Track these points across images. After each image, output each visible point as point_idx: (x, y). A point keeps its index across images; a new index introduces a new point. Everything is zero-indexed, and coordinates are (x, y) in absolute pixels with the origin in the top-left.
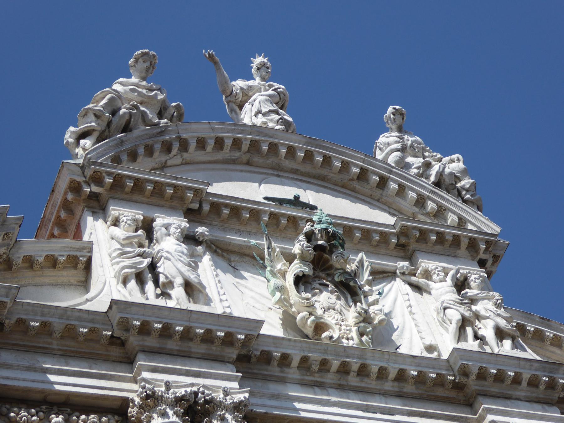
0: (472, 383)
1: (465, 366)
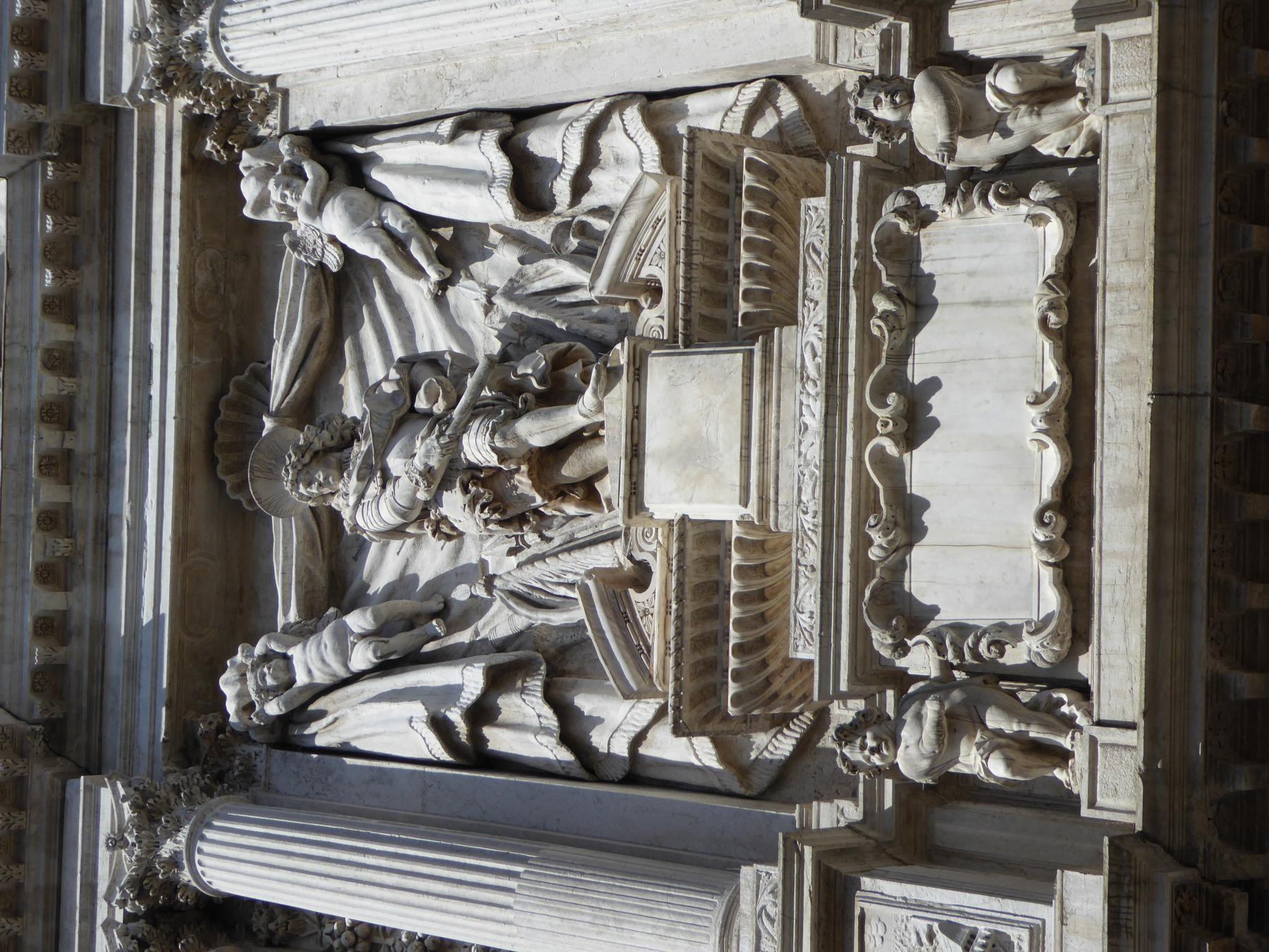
0: (55, 114)
1: (13, 136)
